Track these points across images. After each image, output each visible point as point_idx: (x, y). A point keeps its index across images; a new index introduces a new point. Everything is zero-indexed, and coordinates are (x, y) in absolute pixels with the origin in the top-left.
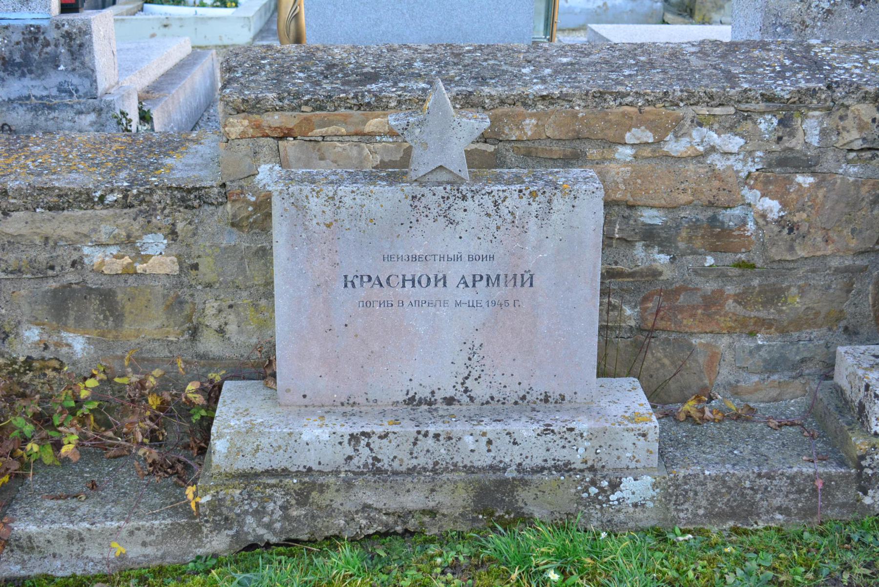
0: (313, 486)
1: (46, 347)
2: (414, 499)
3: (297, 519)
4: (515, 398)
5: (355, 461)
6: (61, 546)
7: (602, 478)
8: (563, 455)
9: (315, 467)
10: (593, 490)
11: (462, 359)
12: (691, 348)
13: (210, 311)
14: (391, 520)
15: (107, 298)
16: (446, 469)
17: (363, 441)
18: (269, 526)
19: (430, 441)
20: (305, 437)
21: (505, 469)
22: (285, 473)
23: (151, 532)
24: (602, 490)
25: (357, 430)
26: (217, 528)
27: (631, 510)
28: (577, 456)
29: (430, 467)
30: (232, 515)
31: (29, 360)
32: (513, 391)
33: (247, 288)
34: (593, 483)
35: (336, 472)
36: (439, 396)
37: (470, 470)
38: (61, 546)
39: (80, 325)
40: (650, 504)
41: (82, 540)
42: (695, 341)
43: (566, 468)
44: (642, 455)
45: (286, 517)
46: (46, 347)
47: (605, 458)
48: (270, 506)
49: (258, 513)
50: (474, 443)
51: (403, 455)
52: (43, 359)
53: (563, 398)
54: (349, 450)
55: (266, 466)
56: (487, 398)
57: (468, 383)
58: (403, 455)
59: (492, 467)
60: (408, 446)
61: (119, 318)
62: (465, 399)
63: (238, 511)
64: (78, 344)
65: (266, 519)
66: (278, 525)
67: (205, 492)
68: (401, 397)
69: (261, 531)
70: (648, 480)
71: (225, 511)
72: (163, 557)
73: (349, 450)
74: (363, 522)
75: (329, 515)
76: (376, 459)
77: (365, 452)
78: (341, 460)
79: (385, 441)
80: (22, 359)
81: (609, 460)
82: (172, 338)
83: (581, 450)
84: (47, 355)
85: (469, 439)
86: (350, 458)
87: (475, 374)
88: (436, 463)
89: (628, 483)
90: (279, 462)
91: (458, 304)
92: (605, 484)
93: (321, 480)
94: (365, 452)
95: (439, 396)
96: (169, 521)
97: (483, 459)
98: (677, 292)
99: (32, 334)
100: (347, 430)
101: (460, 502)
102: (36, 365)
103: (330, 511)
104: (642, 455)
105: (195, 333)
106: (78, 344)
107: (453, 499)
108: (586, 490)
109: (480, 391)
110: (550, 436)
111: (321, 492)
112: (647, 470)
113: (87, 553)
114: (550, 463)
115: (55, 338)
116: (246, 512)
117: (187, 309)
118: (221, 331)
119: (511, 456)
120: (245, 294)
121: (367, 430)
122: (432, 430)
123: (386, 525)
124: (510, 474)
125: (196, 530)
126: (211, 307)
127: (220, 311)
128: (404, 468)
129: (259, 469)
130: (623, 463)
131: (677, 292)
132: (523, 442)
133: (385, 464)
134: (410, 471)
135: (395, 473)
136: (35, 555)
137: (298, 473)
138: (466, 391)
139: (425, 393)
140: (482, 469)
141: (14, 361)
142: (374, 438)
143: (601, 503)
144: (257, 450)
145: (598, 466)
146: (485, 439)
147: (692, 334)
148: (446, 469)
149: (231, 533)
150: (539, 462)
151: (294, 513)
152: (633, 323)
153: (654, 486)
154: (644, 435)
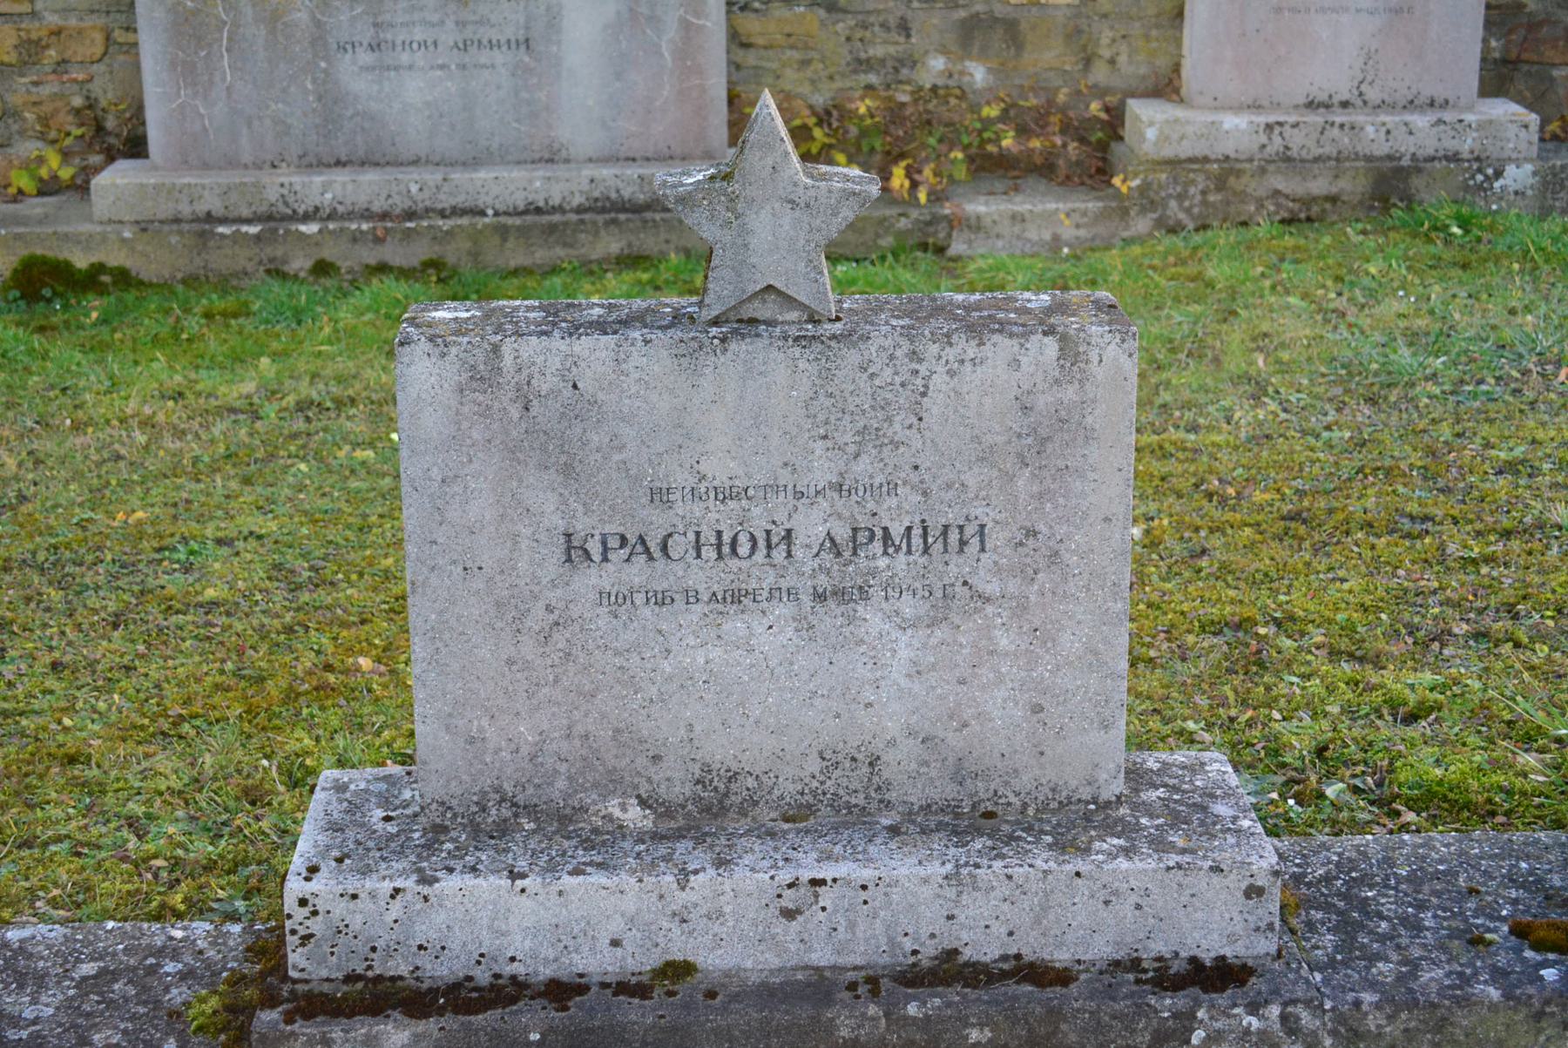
0: (1231, 171)
1: (951, 76)
2: (1319, 186)
3: (1213, 205)
4: (1404, 102)
5: (1268, 149)
6: (1005, 228)
7: (1485, 167)
8: (1451, 145)
9: (1233, 155)
10: (1480, 177)
11: (1359, 63)
12: (1552, 80)
13: (1105, 41)
14: (1296, 206)
15: (1011, 30)
16: (1348, 159)
17: (1277, 130)
18: (1188, 211)
19: (1336, 131)
20: (1226, 126)
21: (1400, 159)
22: (1206, 160)
23: (1084, 214)
24: (1487, 177)
25: (1272, 119)
26: (1143, 211)
27: (1512, 197)
28: (1467, 144)
29: (1334, 155)
30: (1157, 198)
31: (934, 89)
32: (1403, 95)
33: (1140, 18)
34: (1480, 170)
35: (1251, 160)
36: (1336, 100)
37: (1369, 159)
38: (1005, 228)
39: (983, 55)
40: (1530, 192)
41: (1024, 220)
42: (1555, 73)
43: (1455, 158)
44: (1523, 146)
45: (1204, 203)
46: (951, 76)
47: (1491, 148)
48: (1192, 190)
49: (1181, 197)
50: (1375, 135)
51: (1311, 143)
52: (947, 87)
53: (1447, 102)
54: (1263, 139)
55: (1189, 153)
56: (1378, 101)
57: (1363, 88)
58: (1311, 143)
59: (1390, 157)
60: (1315, 135)
61: (1020, 47)
62: (1359, 102)
63: (1163, 194)
64: (979, 74)
65: (1187, 204)
66: (1196, 210)
67: (1136, 175)
68: (1302, 100)
69: (1182, 216)
70: (1529, 167)
71: (1152, 194)
72: (1093, 239)
73: (1263, 139)
74: (1272, 208)
75: (1243, 202)
76: (1287, 148)
77: (1277, 140)
78: (1256, 147)
79: (1296, 131)
80: (928, 86)
81: (1493, 151)
82: (1068, 68)
83: (1469, 141)
84: (951, 83)
85: (1370, 129)
86: (1264, 146)
87: (1369, 78)
88: (1340, 152)
89: (1511, 170)
90: (1200, 150)
91: (1358, 11)
92: (1490, 171)
93: (1238, 166)
94: (1277, 140)
95: (1336, 100)
96: (1100, 204)
97: (1381, 149)
98: (1541, 24)
99: (938, 63)
100: (1262, 119)
101: (1360, 189)
102: (941, 92)
103: (1242, 196)
104: (1523, 146)
105: (1088, 62)
106: (979, 74)
107: (1352, 185)
108: (1473, 177)
109: (1373, 95)
110: (1442, 127)
111: (1238, 177)
112: (1526, 160)
113: (1028, 235)
114: (1441, 153)
115: (959, 67)
116: (1170, 196)
117: (1085, 37)
118: (1112, 62)
119: (1406, 146)
120: (1137, 25)
121: (1281, 119)
122: (1338, 120)
123: (1291, 211)
124: (1405, 162)
125: (1124, 213)
126: (1106, 36)
127: (1114, 41)
128: (1310, 157)
129: (1183, 156)
130: (1505, 155)
131: (1541, 24)
132: (1420, 134)
133: (1294, 153)
134: (1317, 160)
135: (1303, 161)
136: (982, 235)
137: (1217, 161)
138: (1361, 94)
139: (1323, 97)
140: (1381, 159)
141: (921, 89)
142: (1287, 127)
143: (1485, 190)
144: (1182, 138)
145: (1483, 156)
146: (1384, 129)
147: (1554, 65)
148: (1348, 159)
149: (1155, 216)
150: (1431, 152)
151: (1211, 198)
152: (1497, 55)
153: (1535, 173)
154: (1526, 127)
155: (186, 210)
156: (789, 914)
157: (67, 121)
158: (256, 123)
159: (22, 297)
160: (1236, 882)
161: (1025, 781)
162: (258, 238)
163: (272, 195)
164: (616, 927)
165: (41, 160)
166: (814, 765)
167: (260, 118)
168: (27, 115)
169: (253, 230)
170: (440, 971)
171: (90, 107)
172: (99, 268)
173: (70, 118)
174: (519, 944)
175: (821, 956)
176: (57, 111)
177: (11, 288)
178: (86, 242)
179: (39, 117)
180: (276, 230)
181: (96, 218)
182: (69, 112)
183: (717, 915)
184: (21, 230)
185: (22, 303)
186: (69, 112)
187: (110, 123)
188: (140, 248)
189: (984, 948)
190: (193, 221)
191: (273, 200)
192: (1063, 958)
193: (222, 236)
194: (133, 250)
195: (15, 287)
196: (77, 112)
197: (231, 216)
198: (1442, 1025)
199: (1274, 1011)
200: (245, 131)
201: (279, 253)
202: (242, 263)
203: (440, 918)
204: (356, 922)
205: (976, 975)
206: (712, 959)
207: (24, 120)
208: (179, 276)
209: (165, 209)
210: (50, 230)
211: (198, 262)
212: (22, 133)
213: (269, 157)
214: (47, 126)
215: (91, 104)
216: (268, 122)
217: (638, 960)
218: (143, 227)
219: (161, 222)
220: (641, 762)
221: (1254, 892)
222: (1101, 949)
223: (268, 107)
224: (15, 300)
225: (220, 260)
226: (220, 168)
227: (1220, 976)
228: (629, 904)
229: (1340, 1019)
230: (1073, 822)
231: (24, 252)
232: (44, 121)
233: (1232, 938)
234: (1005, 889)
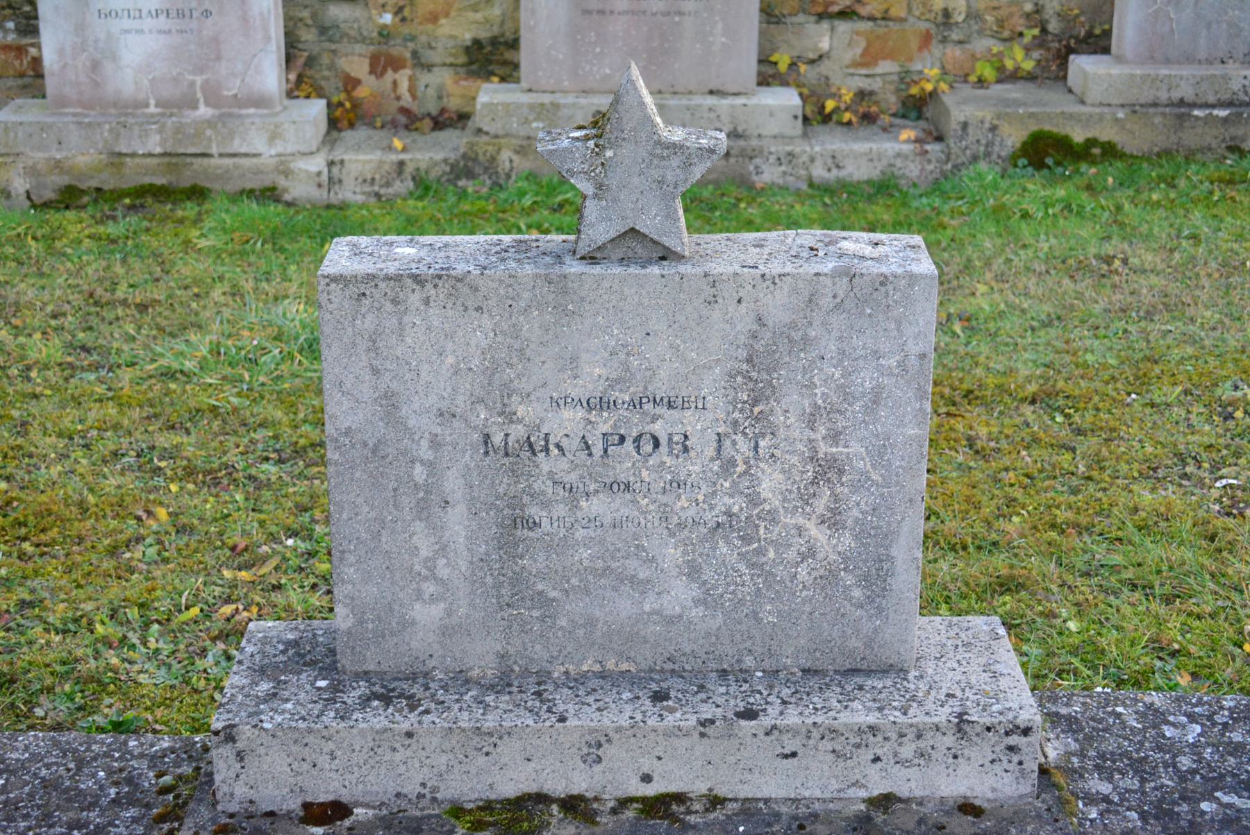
155: (1163, 96)
157: (1019, 24)
158: (1214, 26)
159: (1030, 164)
162: (1225, 120)
163: (1236, 85)
165: (1000, 55)
167: (1218, 22)
168: (988, 18)
169: (1223, 113)
171: (1037, 12)
172: (1091, 142)
173: (1022, 21)
176: (1011, 15)
177: (1019, 157)
178: (1087, 121)
179: (997, 20)
180: (1241, 114)
181: (1088, 101)
182: (1021, 16)
184: (1031, 110)
185: (1030, 169)
186: (1021, 16)
187: (1054, 26)
188: (1128, 126)
190: (1167, 106)
191: (1236, 89)
193: (1197, 118)
194: (1123, 128)
195: (1024, 156)
196: (1028, 16)
197: (1199, 102)
200: (1204, 32)
201: (1240, 132)
202: (1209, 139)
207: (984, 21)
208: (1156, 149)
209: (1147, 95)
210: (1059, 111)
211: (1174, 138)
212: (980, 32)
213: (1221, 54)
214: (1002, 27)
215: (1038, 10)
216: (1224, 26)
218: (1133, 108)
219: (1142, 106)
223: (1226, 13)
224: (1025, 167)
225: (1190, 138)
226: (1179, 63)
231: (1034, 128)
232: (1001, 23)
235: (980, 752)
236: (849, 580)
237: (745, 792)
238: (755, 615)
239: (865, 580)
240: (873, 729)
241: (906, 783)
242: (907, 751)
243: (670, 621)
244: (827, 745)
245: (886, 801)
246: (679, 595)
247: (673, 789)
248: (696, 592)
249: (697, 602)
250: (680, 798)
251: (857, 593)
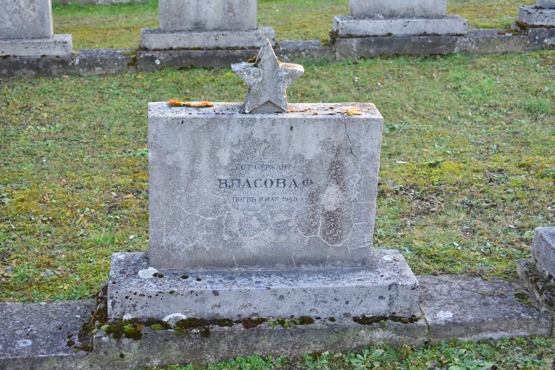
156: (405, 26)
160: (462, 23)
161: (433, 13)
164: (382, 27)
166: (405, 10)
170: (359, 34)
174: (369, 30)
175: (409, 33)
183: (395, 26)
189: (429, 32)
192: (439, 33)
198: (489, 41)
199: (468, 38)
203: (359, 26)
204: (349, 26)
205: (428, 35)
206: (394, 33)
217: (385, 33)
220: (383, 9)
221: (465, 24)
222: (445, 32)
227: (461, 35)
228: (384, 24)
229: (476, 40)
230: (440, 17)
233: (462, 31)
234: (433, 23)
235: (59, 46)
236: (38, 21)
237: (20, 55)
238: (22, 28)
239: (41, 21)
240: (40, 43)
241: (47, 53)
242: (46, 47)
243: (8, 29)
244: (33, 46)
245: (43, 56)
246: (9, 24)
247: (8, 54)
248: (12, 23)
249: (12, 25)
250: (9, 56)
251: (40, 23)
